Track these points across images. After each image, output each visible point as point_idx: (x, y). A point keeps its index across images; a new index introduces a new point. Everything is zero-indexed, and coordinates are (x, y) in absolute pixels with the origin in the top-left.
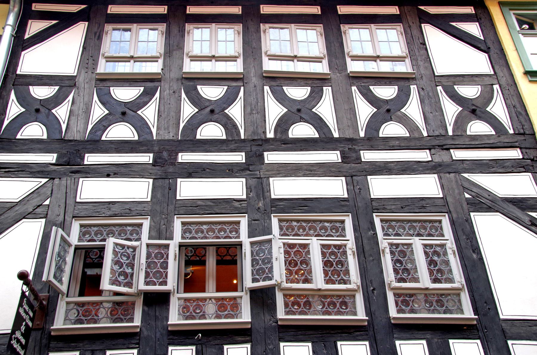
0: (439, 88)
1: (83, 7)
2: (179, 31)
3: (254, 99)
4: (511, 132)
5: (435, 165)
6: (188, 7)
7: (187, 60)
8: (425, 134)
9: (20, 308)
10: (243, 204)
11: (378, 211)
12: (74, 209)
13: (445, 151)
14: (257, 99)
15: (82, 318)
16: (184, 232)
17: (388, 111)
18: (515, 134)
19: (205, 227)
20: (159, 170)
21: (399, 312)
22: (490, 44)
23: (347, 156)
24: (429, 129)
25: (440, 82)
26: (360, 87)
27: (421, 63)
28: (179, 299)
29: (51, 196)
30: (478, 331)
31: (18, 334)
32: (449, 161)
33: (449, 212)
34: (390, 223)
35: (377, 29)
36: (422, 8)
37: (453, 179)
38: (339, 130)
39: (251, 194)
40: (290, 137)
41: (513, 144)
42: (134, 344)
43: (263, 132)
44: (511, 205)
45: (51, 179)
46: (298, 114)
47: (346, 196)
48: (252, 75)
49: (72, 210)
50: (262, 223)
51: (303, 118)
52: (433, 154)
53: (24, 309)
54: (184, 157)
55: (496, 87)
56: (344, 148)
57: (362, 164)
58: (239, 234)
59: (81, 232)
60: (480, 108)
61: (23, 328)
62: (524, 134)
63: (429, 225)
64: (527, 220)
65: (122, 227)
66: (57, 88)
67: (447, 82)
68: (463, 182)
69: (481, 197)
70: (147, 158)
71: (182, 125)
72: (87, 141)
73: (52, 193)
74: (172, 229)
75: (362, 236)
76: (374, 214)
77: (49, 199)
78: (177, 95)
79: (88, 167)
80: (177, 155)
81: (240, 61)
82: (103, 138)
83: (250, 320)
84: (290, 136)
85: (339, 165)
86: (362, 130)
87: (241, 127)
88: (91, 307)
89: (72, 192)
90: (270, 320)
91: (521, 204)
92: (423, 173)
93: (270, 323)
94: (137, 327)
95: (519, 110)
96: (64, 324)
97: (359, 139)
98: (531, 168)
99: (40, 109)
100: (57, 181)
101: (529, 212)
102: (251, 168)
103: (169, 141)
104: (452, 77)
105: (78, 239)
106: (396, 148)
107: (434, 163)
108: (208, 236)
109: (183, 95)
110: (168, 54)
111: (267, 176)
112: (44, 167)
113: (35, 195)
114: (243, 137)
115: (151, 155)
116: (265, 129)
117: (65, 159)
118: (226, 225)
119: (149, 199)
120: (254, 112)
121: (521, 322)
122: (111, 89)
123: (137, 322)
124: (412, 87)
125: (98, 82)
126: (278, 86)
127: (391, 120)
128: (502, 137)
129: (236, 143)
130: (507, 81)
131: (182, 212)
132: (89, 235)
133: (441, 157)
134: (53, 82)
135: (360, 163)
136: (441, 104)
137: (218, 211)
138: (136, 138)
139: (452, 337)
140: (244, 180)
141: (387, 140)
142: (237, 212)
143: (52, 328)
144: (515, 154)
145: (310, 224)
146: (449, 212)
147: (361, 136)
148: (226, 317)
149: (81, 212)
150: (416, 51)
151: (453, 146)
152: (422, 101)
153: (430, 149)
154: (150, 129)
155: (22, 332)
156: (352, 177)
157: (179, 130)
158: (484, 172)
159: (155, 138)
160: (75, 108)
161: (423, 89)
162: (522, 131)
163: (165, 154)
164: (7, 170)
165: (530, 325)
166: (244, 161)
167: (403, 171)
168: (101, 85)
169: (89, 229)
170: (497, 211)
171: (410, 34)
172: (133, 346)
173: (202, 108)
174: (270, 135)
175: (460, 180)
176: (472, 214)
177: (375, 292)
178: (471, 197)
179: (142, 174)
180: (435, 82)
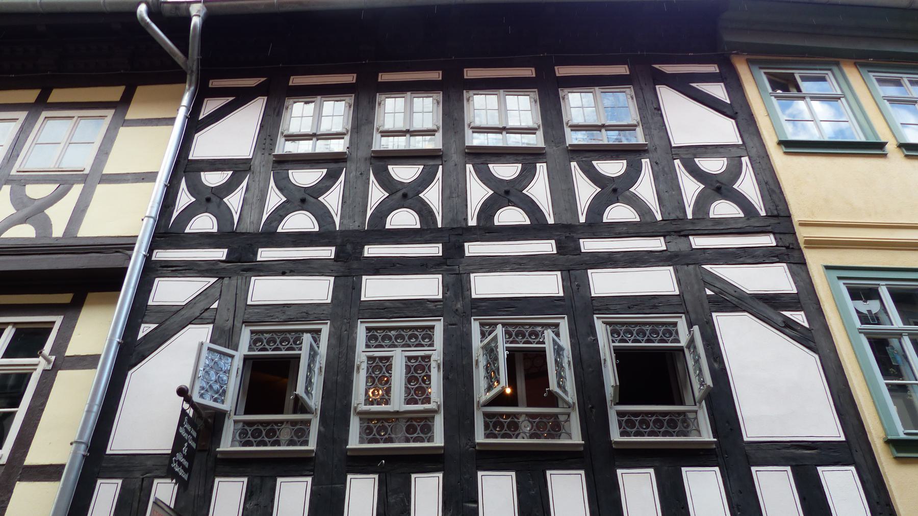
0: (677, 162)
1: (263, 79)
2: (369, 102)
3: (454, 180)
4: (763, 213)
6: (380, 74)
7: (377, 136)
8: (659, 218)
9: (181, 428)
10: (438, 305)
11: (600, 312)
12: (245, 313)
13: (683, 239)
14: (458, 179)
15: (251, 439)
16: (369, 339)
17: (615, 190)
19: (393, 333)
20: (341, 267)
21: (623, 434)
22: (737, 109)
23: (564, 245)
24: (664, 211)
25: (678, 154)
26: (581, 162)
27: (655, 132)
29: (220, 298)
30: (717, 457)
31: (179, 457)
32: (687, 250)
33: (686, 312)
35: (602, 92)
36: (657, 66)
37: (692, 272)
38: (554, 214)
39: (449, 293)
40: (495, 224)
41: (763, 229)
42: (308, 470)
43: (464, 219)
44: (761, 303)
45: (220, 278)
46: (506, 196)
47: (561, 294)
48: (453, 151)
49: (242, 314)
50: (460, 328)
51: (513, 202)
52: (668, 242)
53: (185, 428)
54: (372, 251)
55: (745, 160)
56: (560, 237)
57: (581, 256)
58: (433, 341)
59: (252, 339)
60: (726, 185)
61: (185, 450)
62: (777, 216)
63: (662, 329)
64: (779, 320)
65: (298, 333)
66: (231, 173)
68: (704, 276)
69: (725, 293)
70: (327, 252)
71: (369, 213)
72: (261, 233)
73: (220, 295)
74: (354, 335)
75: (580, 342)
76: (595, 316)
77: (218, 301)
78: (364, 177)
80: (363, 248)
81: (439, 135)
82: (279, 230)
83: (442, 445)
84: (496, 223)
86: (582, 214)
87: (439, 213)
88: (260, 427)
89: (243, 293)
90: (467, 444)
91: (773, 302)
93: (466, 448)
94: (312, 451)
95: (773, 187)
96: (232, 446)
97: (579, 225)
98: (786, 257)
99: (211, 198)
100: (226, 280)
101: (783, 311)
102: (449, 262)
103: (354, 231)
104: (692, 148)
105: (249, 348)
107: (669, 253)
108: (396, 343)
109: (372, 177)
110: (356, 130)
111: (467, 272)
112: (213, 264)
113: (202, 297)
114: (440, 226)
115: (333, 249)
116: (467, 215)
117: (236, 255)
118: (419, 330)
119: (329, 301)
120: (454, 196)
121: (768, 445)
122: (290, 172)
123: (312, 446)
124: (643, 161)
125: (276, 165)
126: (482, 164)
128: (753, 220)
129: (431, 233)
130: (758, 152)
132: (260, 343)
133: (678, 245)
134: (225, 166)
135: (579, 254)
136: (678, 181)
137: (410, 314)
138: (317, 229)
140: (440, 276)
141: (612, 226)
143: (218, 449)
144: (768, 241)
145: (517, 329)
146: (686, 313)
147: (581, 222)
148: (415, 440)
149: (252, 316)
150: (649, 117)
151: (693, 232)
152: (656, 178)
153: (664, 236)
154: (332, 217)
155: (184, 455)
156: (569, 271)
158: (730, 263)
159: (338, 229)
160: (249, 195)
161: (657, 163)
162: (775, 213)
164: (174, 269)
166: (441, 254)
167: (631, 263)
169: (261, 336)
170: (744, 311)
171: (642, 98)
173: (394, 191)
174: (472, 222)
175: (701, 273)
176: (714, 315)
177: (594, 410)
178: (713, 293)
179: (322, 271)
180: (672, 154)
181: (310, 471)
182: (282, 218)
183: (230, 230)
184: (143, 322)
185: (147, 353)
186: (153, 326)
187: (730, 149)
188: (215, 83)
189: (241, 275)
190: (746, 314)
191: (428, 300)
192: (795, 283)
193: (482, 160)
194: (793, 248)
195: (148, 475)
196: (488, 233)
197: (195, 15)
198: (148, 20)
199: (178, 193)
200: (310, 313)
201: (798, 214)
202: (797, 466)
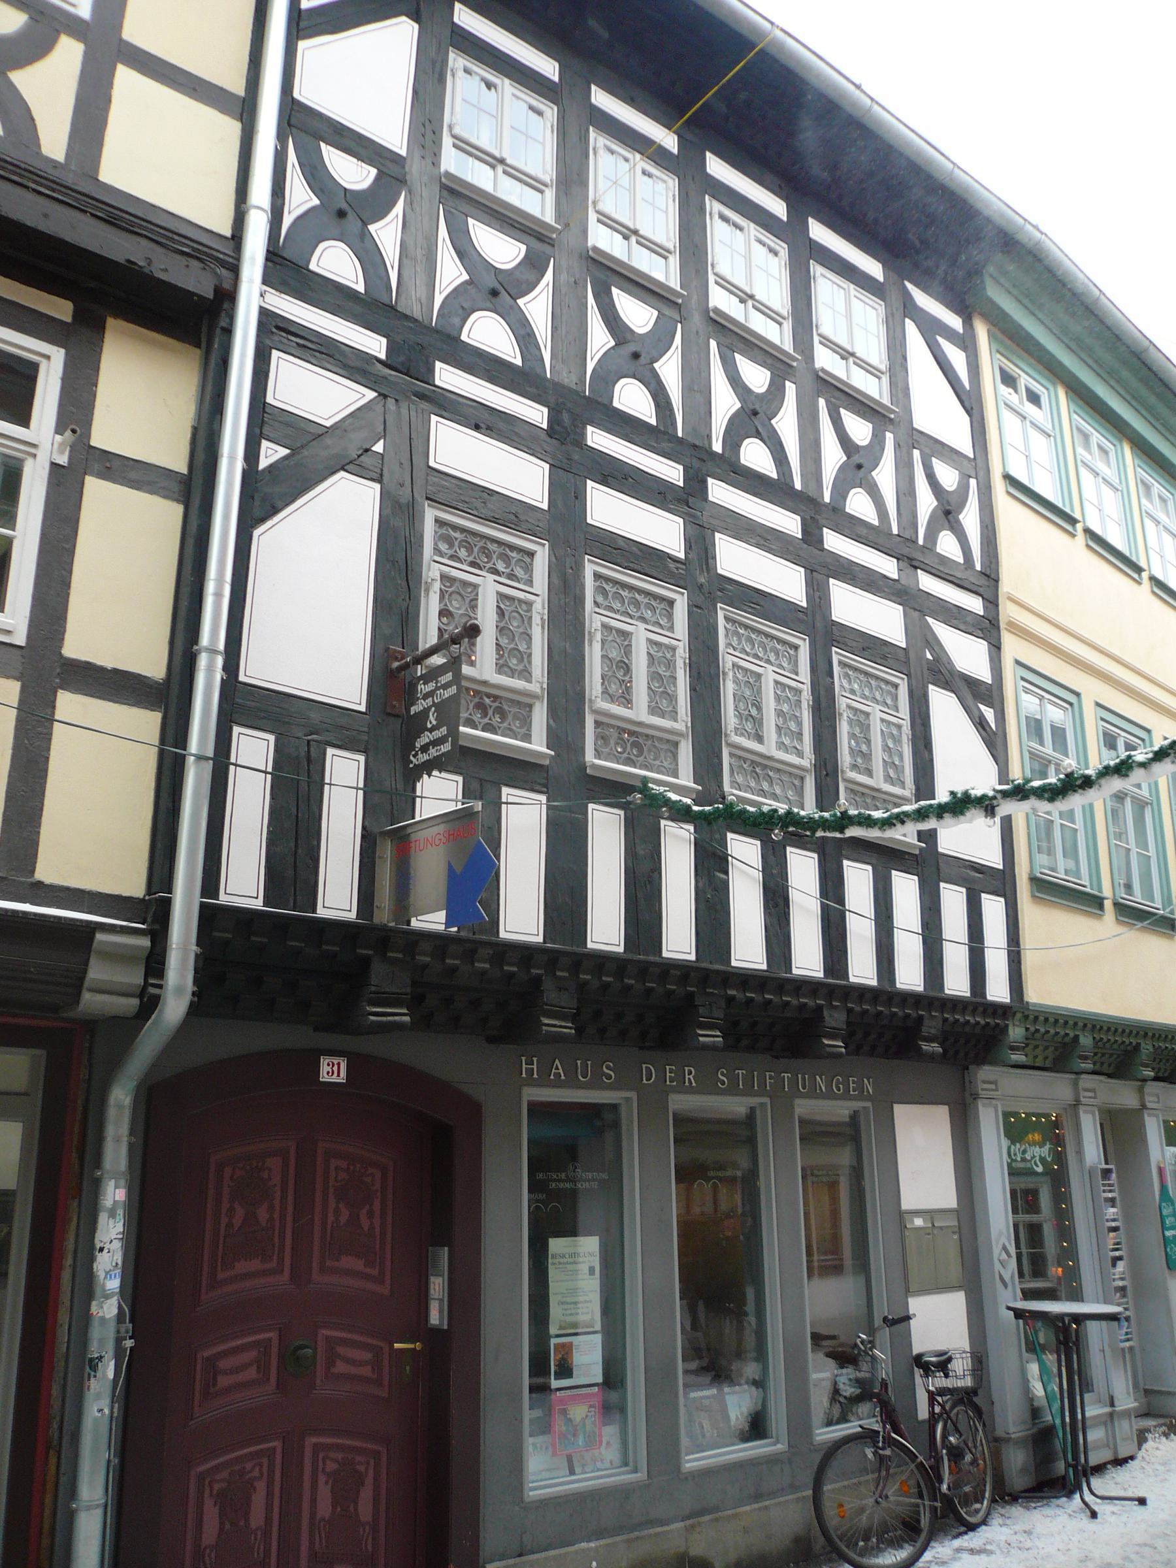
4: (978, 567)
42: (540, 784)
64: (976, 713)
71: (590, 366)
79: (443, 395)
100: (391, 403)
107: (900, 586)
144: (974, 604)
151: (922, 566)
153: (898, 559)
157: (585, 373)
162: (988, 573)
170: (953, 691)
172: (538, 787)
176: (931, 687)
185: (279, 504)
189: (414, 402)
190: (954, 695)
195: (314, 737)
199: (285, 170)
201: (1007, 585)
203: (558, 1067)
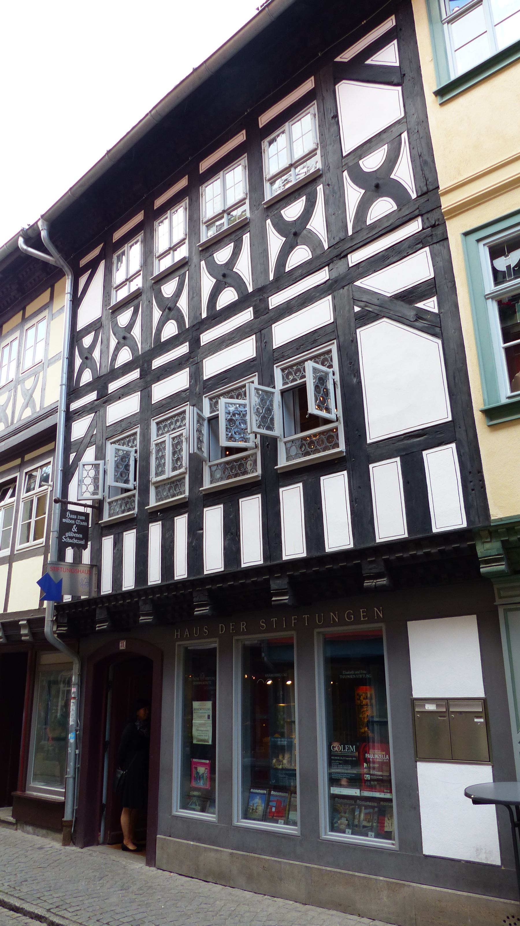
1: (102, 245)
5: (332, 283)
16: (158, 429)
18: (418, 197)
26: (273, 217)
28: (285, 443)
30: (346, 462)
34: (289, 370)
54: (157, 363)
66: (93, 333)
67: (354, 159)
69: (369, 305)
72: (109, 373)
78: (151, 304)
85: (251, 323)
91: (411, 296)
92: (319, 299)
97: (269, 284)
98: (429, 239)
101: (417, 303)
102: (192, 355)
104: (357, 150)
106: (298, 279)
107: (330, 281)
112: (92, 404)
114: (187, 327)
120: (195, 295)
127: (297, 245)
129: (184, 334)
131: (155, 414)
137: (173, 406)
139: (323, 474)
141: (291, 274)
142: (183, 402)
151: (350, 250)
156: (260, 331)
163: (146, 365)
165: (393, 442)
168: (113, 317)
170: (383, 317)
175: (353, 291)
181: (136, 525)
182: (116, 356)
183: (96, 377)
184: (70, 454)
186: (75, 454)
187: (391, 130)
188: (83, 262)
190: (385, 319)
191: (182, 391)
192: (434, 266)
193: (210, 252)
194: (438, 225)
196: (214, 319)
197: (42, 230)
198: (25, 247)
200: (131, 422)
202: (406, 454)
203: (187, 632)
